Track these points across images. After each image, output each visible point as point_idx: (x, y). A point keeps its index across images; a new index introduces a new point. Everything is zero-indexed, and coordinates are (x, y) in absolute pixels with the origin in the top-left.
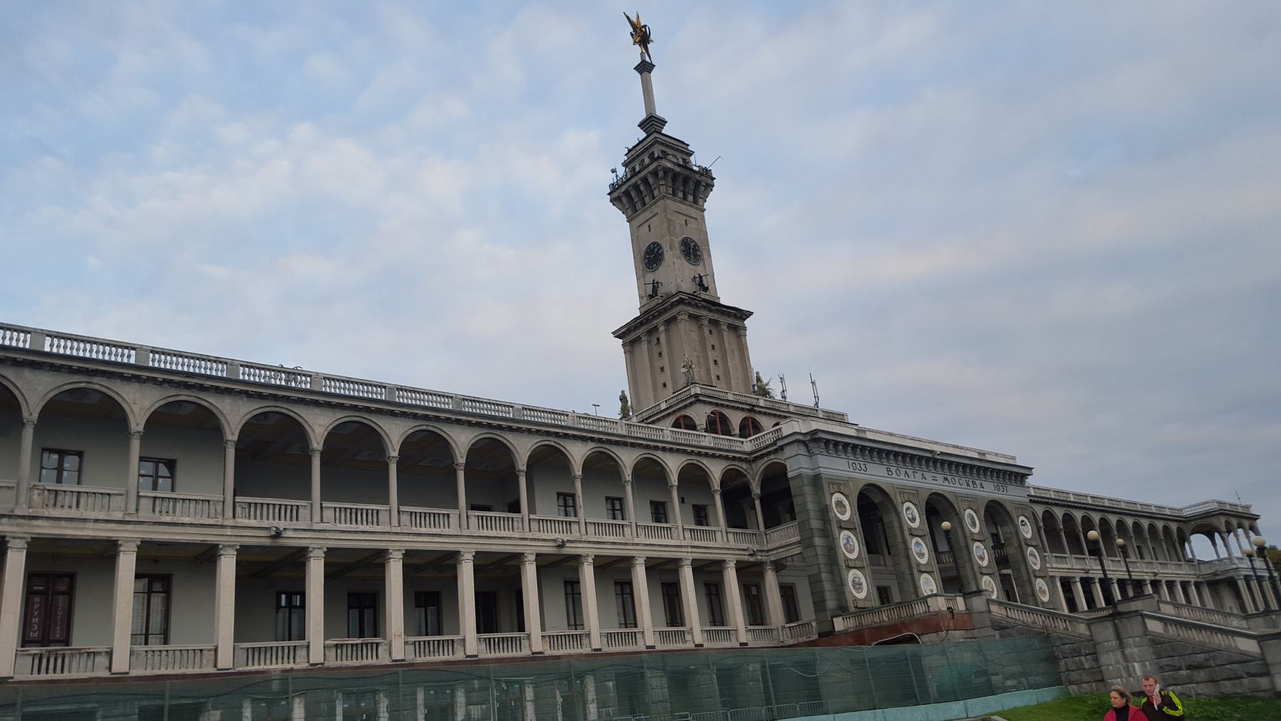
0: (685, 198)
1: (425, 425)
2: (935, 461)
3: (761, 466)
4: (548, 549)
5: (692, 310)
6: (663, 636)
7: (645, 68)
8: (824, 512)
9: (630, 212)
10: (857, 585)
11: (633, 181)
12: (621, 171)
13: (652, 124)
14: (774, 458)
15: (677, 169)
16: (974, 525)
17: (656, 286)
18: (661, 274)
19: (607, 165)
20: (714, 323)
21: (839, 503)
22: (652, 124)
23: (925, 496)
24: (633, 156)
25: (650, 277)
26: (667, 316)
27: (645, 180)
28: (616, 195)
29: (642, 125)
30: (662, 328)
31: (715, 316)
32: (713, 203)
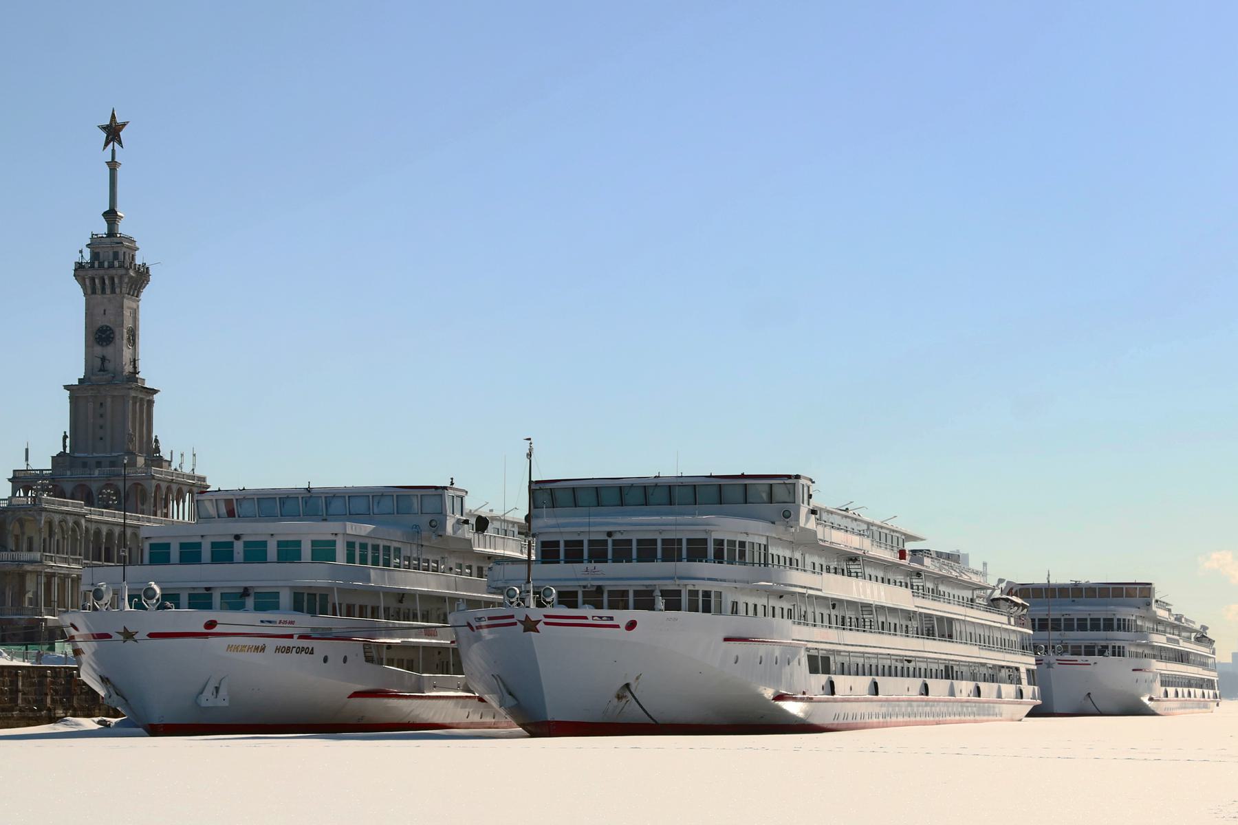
7: (113, 165)
9: (89, 291)
11: (101, 272)
12: (87, 257)
13: (111, 216)
17: (103, 359)
18: (109, 351)
19: (77, 249)
22: (111, 216)
24: (95, 243)
25: (98, 350)
27: (112, 279)
28: (81, 273)
29: (106, 214)
30: (109, 400)
32: (146, 294)
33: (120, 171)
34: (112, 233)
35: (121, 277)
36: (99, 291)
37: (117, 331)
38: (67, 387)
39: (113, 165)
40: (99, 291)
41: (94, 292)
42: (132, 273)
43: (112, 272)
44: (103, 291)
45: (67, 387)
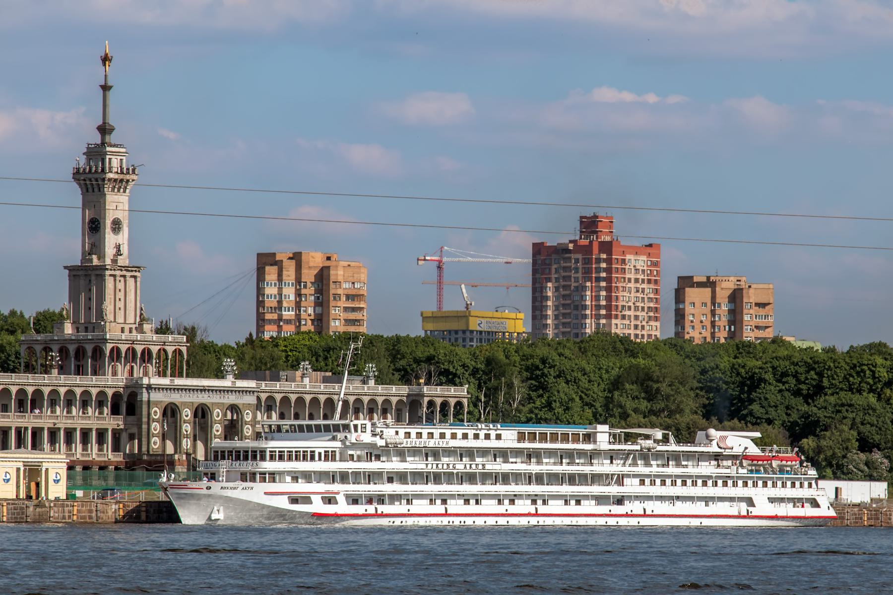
0: (119, 191)
1: (21, 387)
2: (205, 390)
3: (129, 391)
4: (51, 426)
5: (112, 272)
6: (83, 455)
7: (106, 88)
8: (149, 414)
9: (85, 190)
10: (155, 443)
11: (90, 176)
12: (82, 160)
14: (134, 389)
15: (116, 176)
16: (218, 416)
20: (124, 276)
21: (155, 412)
22: (104, 130)
23: (195, 406)
26: (98, 272)
28: (77, 176)
31: (124, 273)
33: (111, 94)
34: (103, 143)
35: (104, 180)
36: (90, 190)
37: (101, 221)
38: (65, 268)
39: (106, 88)
40: (90, 190)
41: (87, 191)
42: (111, 175)
43: (96, 176)
44: (93, 191)
45: (65, 268)
